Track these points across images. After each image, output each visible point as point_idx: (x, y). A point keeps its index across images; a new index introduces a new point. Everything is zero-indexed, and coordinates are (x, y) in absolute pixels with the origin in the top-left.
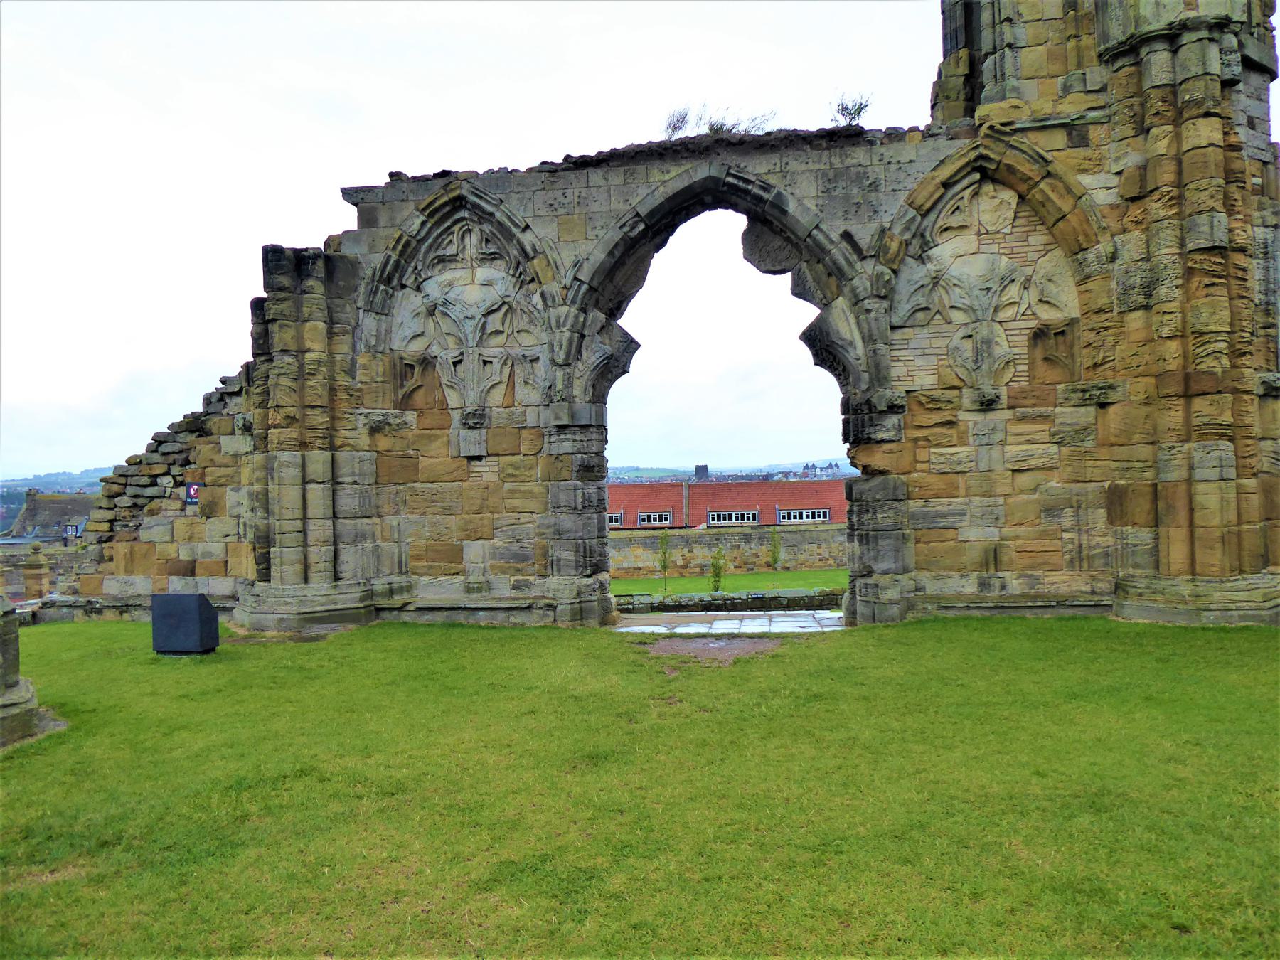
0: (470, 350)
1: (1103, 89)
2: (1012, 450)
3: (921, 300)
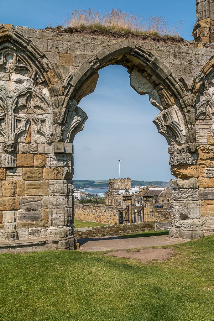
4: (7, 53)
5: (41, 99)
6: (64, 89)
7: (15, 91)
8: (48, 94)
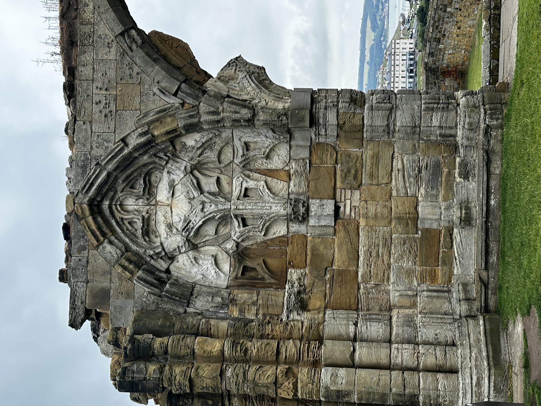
0: (233, 207)
4: (119, 209)
5: (205, 149)
6: (186, 105)
7: (192, 197)
8: (197, 136)
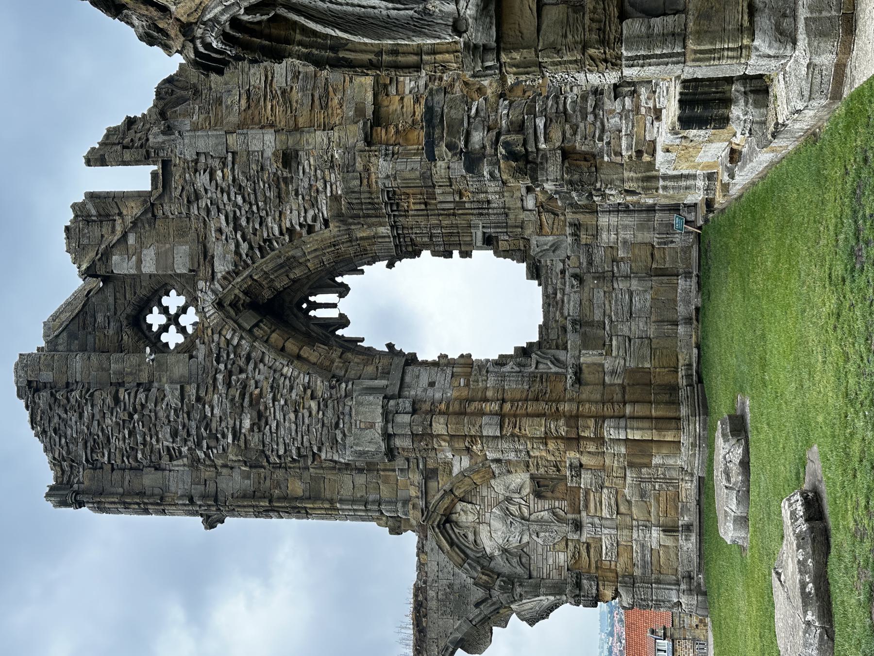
1: (408, 460)
2: (605, 513)
3: (514, 561)
